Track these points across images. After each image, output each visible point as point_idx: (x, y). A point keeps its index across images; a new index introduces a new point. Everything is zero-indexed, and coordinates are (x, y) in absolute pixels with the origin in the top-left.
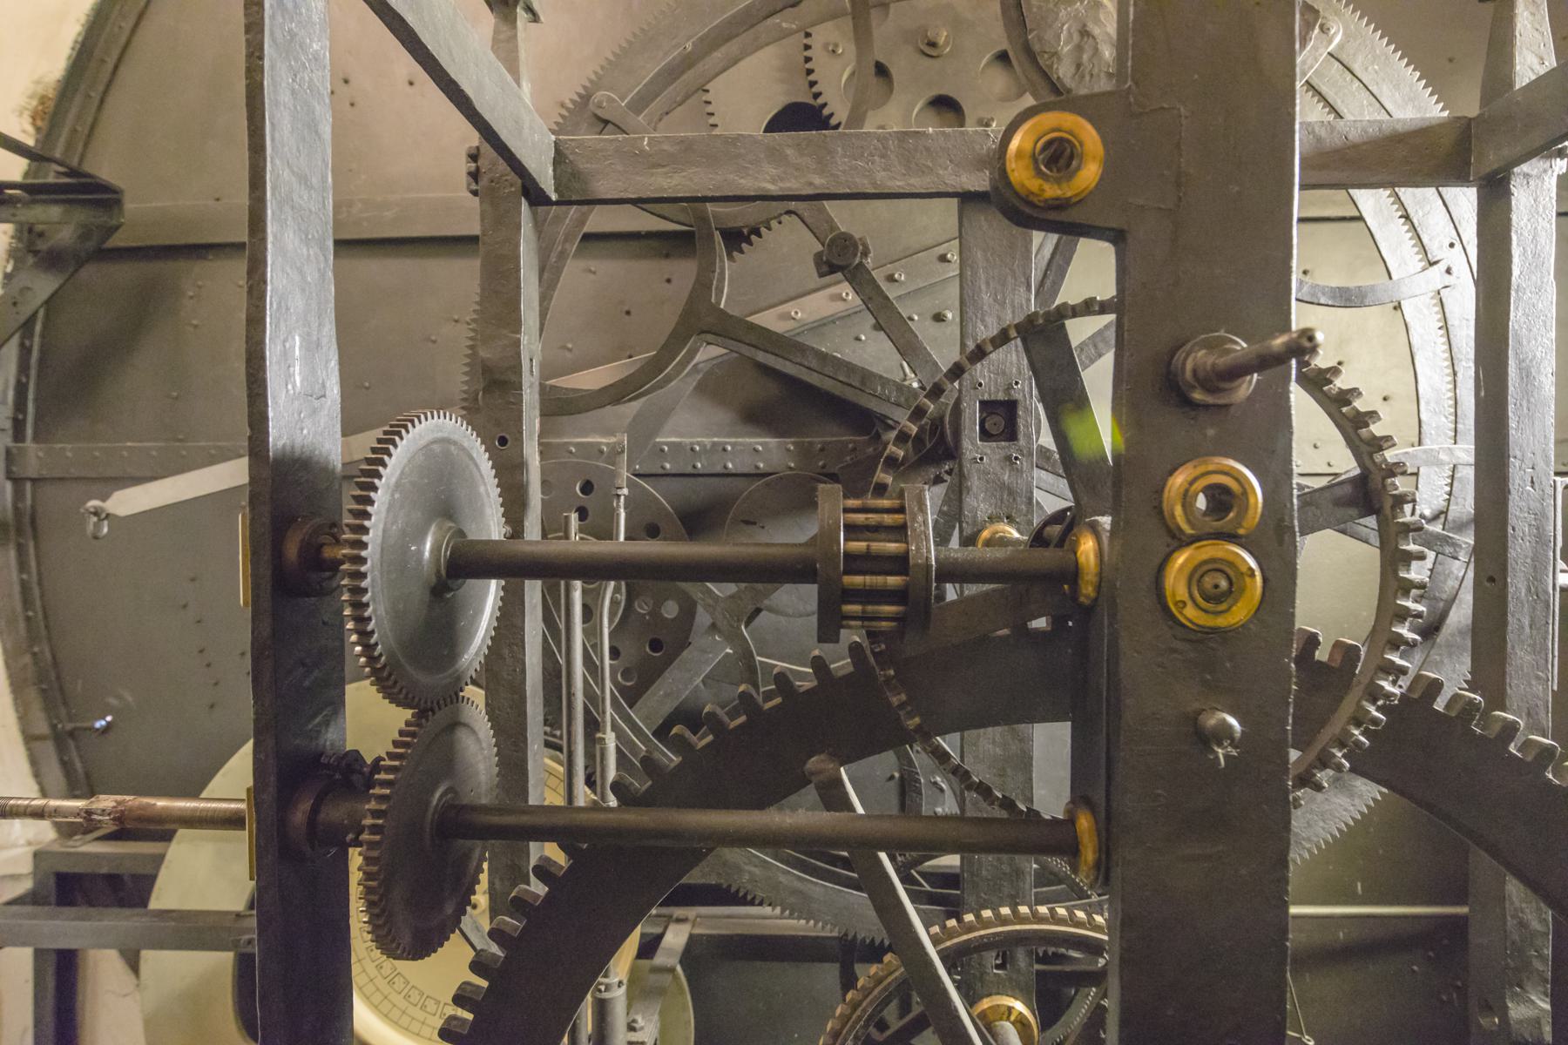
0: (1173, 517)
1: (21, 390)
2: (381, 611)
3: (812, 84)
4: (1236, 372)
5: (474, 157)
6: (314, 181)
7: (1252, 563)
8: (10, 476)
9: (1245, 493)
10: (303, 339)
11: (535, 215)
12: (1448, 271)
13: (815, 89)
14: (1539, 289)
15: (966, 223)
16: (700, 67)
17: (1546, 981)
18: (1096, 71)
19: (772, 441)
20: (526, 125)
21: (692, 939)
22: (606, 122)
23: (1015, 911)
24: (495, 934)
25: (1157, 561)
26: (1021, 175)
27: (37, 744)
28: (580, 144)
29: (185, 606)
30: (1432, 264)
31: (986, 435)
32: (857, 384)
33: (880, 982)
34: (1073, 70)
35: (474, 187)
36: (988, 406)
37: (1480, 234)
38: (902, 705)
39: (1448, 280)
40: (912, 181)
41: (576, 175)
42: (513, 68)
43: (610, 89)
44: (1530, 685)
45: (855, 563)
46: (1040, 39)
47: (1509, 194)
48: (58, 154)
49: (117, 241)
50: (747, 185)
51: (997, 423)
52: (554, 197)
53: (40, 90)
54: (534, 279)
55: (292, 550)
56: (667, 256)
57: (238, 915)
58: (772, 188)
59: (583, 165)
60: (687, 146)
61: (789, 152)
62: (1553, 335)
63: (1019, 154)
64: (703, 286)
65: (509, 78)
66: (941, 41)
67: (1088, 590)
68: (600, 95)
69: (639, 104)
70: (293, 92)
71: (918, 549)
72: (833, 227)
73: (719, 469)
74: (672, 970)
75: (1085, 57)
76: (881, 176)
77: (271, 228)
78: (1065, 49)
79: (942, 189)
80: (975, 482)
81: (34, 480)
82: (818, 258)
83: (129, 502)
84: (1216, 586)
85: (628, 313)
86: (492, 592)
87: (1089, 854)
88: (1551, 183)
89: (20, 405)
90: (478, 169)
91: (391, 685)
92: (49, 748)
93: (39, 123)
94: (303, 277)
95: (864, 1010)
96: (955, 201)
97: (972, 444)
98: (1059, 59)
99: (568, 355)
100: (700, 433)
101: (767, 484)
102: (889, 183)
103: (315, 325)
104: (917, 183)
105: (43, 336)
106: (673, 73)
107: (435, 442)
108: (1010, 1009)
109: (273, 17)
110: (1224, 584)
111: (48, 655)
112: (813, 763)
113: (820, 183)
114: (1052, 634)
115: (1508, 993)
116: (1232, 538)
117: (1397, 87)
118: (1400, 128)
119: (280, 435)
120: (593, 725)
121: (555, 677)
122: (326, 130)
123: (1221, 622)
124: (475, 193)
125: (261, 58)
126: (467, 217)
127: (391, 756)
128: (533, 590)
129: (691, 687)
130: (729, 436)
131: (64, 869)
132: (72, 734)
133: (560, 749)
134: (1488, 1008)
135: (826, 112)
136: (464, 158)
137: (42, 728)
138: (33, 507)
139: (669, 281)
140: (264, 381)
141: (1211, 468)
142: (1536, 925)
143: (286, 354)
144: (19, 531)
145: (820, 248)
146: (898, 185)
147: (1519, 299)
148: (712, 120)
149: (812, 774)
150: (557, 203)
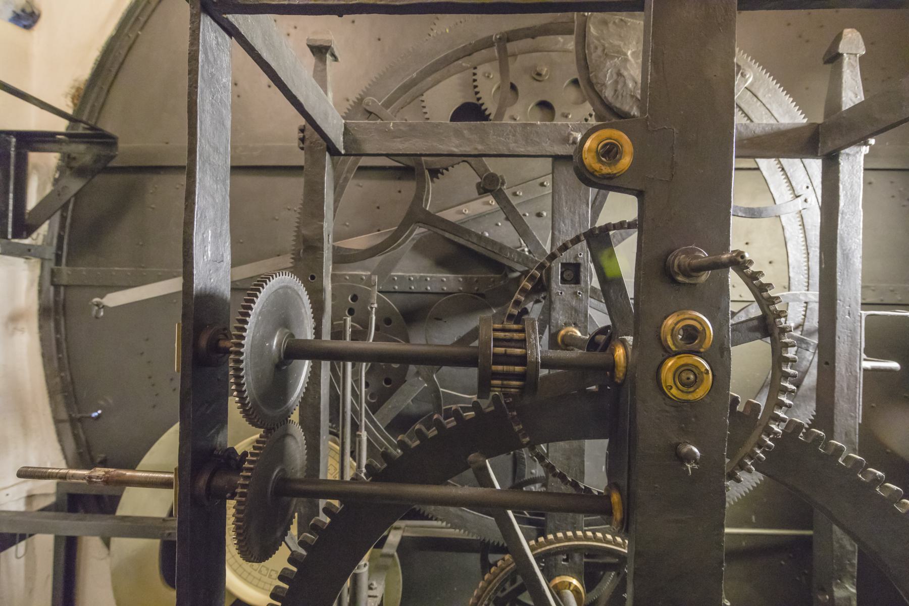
0: (666, 341)
1: (60, 238)
2: (250, 378)
3: (477, 93)
4: (701, 269)
5: (302, 130)
6: (222, 150)
7: (708, 367)
8: (53, 283)
9: (704, 329)
11: (332, 160)
12: (806, 201)
13: (478, 96)
14: (854, 213)
16: (420, 85)
17: (853, 577)
18: (625, 94)
19: (451, 276)
21: (403, 539)
22: (371, 113)
23: (574, 534)
24: (302, 544)
25: (658, 363)
26: (590, 160)
27: (61, 425)
28: (358, 125)
29: (142, 354)
30: (797, 197)
31: (564, 281)
32: (496, 251)
33: (503, 569)
34: (612, 93)
35: (302, 145)
37: (823, 182)
38: (520, 431)
39: (806, 205)
41: (355, 141)
42: (323, 84)
43: (374, 96)
44: (847, 420)
45: (499, 359)
46: (596, 76)
47: (838, 164)
48: (84, 119)
49: (113, 164)
50: (443, 148)
51: (569, 274)
52: (343, 152)
53: (77, 84)
55: (203, 342)
56: (399, 179)
57: (164, 520)
58: (456, 150)
59: (359, 136)
60: (412, 127)
61: (465, 132)
62: (861, 237)
63: (589, 150)
64: (419, 198)
65: (322, 92)
66: (544, 73)
67: (620, 374)
68: (368, 99)
69: (387, 105)
70: (212, 105)
71: (532, 353)
72: (487, 170)
73: (423, 290)
74: (392, 556)
75: (619, 87)
76: (512, 146)
78: (609, 82)
79: (544, 153)
80: (557, 305)
81: (66, 286)
82: (478, 185)
83: (115, 299)
84: (688, 379)
85: (378, 208)
86: (306, 366)
87: (618, 515)
88: (861, 159)
89: (60, 247)
90: (304, 136)
91: (252, 415)
92: (67, 427)
94: (214, 198)
95: (495, 585)
96: (550, 159)
97: (557, 285)
98: (606, 87)
99: (347, 229)
100: (414, 271)
101: (449, 299)
103: (219, 225)
104: (531, 150)
105: (73, 210)
106: (406, 88)
107: (280, 288)
108: (570, 584)
109: (203, 66)
110: (692, 377)
111: (69, 378)
112: (472, 457)
113: (481, 148)
114: (598, 395)
115: (834, 584)
116: (697, 353)
117: (780, 105)
118: (782, 127)
119: (199, 283)
120: (355, 427)
121: (336, 401)
122: (228, 124)
123: (690, 397)
124: (302, 149)
125: (196, 87)
126: (299, 159)
127: (252, 454)
128: (326, 366)
129: (406, 404)
130: (428, 272)
131: (72, 491)
132: (80, 420)
133: (337, 435)
134: (823, 590)
135: (483, 108)
136: (296, 131)
137: (64, 415)
138: (64, 300)
140: (192, 254)
141: (687, 316)
142: (849, 548)
143: (204, 240)
144: (57, 312)
145: (479, 180)
146: (521, 150)
147: (843, 218)
148: (424, 110)
149: (471, 463)
150: (344, 155)
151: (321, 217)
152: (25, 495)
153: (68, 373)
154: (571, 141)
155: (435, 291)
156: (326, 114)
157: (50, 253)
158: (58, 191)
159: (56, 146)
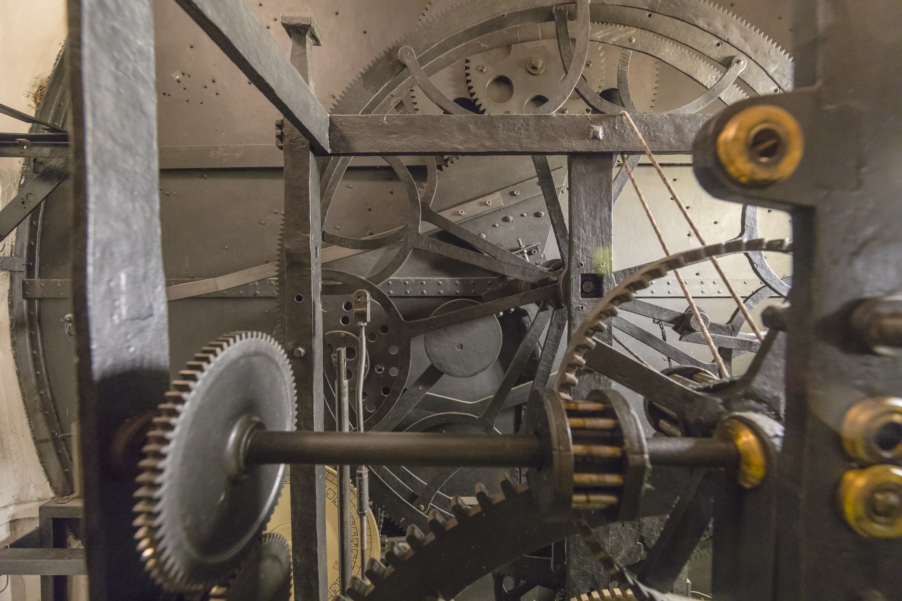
1: (31, 249)
3: (470, 88)
5: (280, 126)
6: (141, 149)
10: (129, 276)
13: (471, 91)
15: (573, 169)
19: (447, 279)
20: (312, 108)
31: (584, 294)
35: (280, 144)
36: (585, 278)
40: (544, 145)
41: (343, 138)
42: (303, 70)
51: (590, 285)
52: (329, 151)
54: (318, 200)
59: (347, 132)
61: (471, 126)
65: (300, 77)
66: (539, 66)
70: (117, 78)
73: (419, 294)
77: (93, 191)
79: (561, 150)
81: (40, 299)
85: (370, 210)
90: (282, 133)
92: (49, 447)
93: (38, 101)
97: (576, 299)
100: (413, 279)
102: (529, 146)
105: (44, 218)
109: (92, 15)
111: (49, 396)
113: (489, 144)
122: (152, 108)
124: (281, 148)
131: (56, 516)
135: (477, 103)
136: (274, 127)
137: (45, 434)
138: (39, 313)
139: (392, 193)
144: (32, 327)
148: (415, 107)
151: (307, 228)
152: (8, 520)
153: (48, 392)
154: (591, 136)
155: (430, 295)
156: (306, 105)
157: (20, 264)
158: (21, 201)
159: (16, 150)
